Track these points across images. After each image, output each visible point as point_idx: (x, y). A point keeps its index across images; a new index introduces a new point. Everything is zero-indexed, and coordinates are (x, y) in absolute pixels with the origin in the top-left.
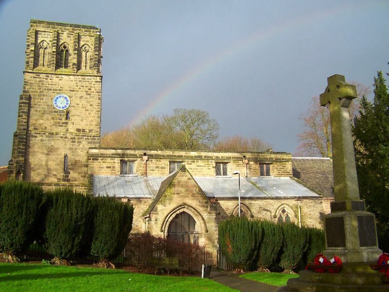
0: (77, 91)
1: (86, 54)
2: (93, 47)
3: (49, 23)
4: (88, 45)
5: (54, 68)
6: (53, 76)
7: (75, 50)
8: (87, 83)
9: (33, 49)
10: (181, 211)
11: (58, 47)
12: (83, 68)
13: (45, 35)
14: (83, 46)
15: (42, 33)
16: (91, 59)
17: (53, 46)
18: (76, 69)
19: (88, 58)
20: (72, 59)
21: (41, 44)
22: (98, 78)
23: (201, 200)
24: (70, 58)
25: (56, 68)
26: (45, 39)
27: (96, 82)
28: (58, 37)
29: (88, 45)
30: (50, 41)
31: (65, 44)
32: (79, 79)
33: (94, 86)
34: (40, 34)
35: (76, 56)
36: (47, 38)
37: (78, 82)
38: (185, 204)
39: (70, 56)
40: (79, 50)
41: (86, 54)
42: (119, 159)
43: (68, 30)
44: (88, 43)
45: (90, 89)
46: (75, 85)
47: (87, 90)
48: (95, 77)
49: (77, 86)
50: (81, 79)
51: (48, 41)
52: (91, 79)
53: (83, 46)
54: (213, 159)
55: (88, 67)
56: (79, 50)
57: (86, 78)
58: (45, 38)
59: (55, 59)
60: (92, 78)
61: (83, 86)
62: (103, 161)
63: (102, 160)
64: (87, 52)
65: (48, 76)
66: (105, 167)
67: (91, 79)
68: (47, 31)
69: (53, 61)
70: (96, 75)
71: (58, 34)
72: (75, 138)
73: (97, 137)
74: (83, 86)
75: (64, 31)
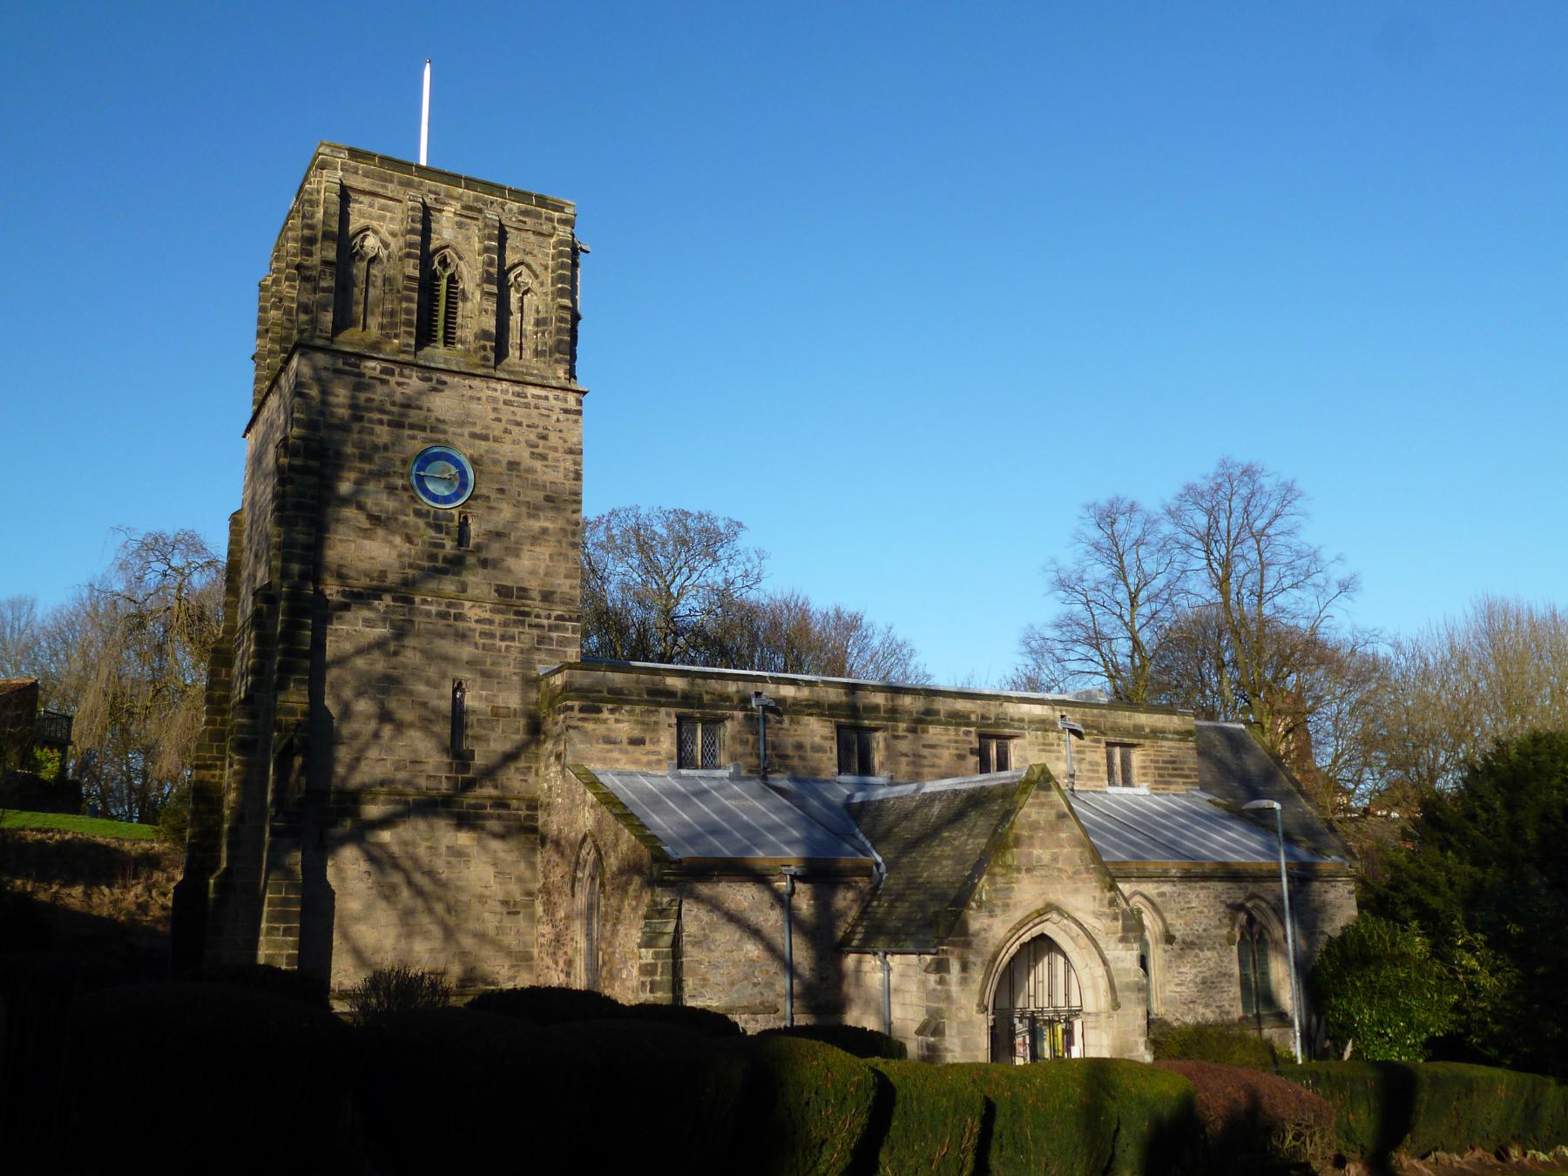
0: (496, 440)
1: (521, 300)
2: (548, 278)
3: (386, 161)
4: (529, 267)
5: (413, 342)
6: (407, 372)
7: (488, 278)
8: (535, 412)
9: (331, 254)
10: (1035, 932)
11: (426, 258)
12: (513, 353)
13: (371, 206)
14: (515, 266)
15: (362, 198)
16: (538, 323)
17: (409, 255)
18: (492, 355)
19: (530, 318)
20: (475, 315)
21: (358, 240)
22: (571, 397)
23: (1098, 894)
24: (463, 308)
25: (420, 345)
26: (375, 224)
27: (566, 411)
28: (426, 216)
29: (529, 267)
30: (393, 235)
31: (447, 251)
32: (505, 392)
33: (560, 426)
34: (356, 201)
35: (491, 306)
36: (382, 218)
37: (501, 405)
38: (1050, 907)
39: (465, 299)
40: (500, 281)
41: (521, 300)
42: (673, 711)
43: (458, 199)
44: (528, 259)
45: (544, 438)
46: (493, 415)
47: (533, 437)
48: (560, 394)
49: (499, 420)
50: (509, 397)
51: (384, 231)
52: (546, 398)
53: (515, 266)
54: (968, 724)
55: (528, 354)
56: (500, 281)
57: (531, 391)
58: (372, 218)
59: (414, 306)
60: (551, 394)
61: (519, 424)
62: (617, 715)
63: (612, 711)
64: (526, 292)
65: (392, 373)
66: (625, 740)
67: (546, 398)
68: (381, 191)
69: (408, 312)
70: (564, 383)
71: (426, 209)
72: (491, 622)
73: (570, 619)
74: (519, 424)
75: (444, 204)
